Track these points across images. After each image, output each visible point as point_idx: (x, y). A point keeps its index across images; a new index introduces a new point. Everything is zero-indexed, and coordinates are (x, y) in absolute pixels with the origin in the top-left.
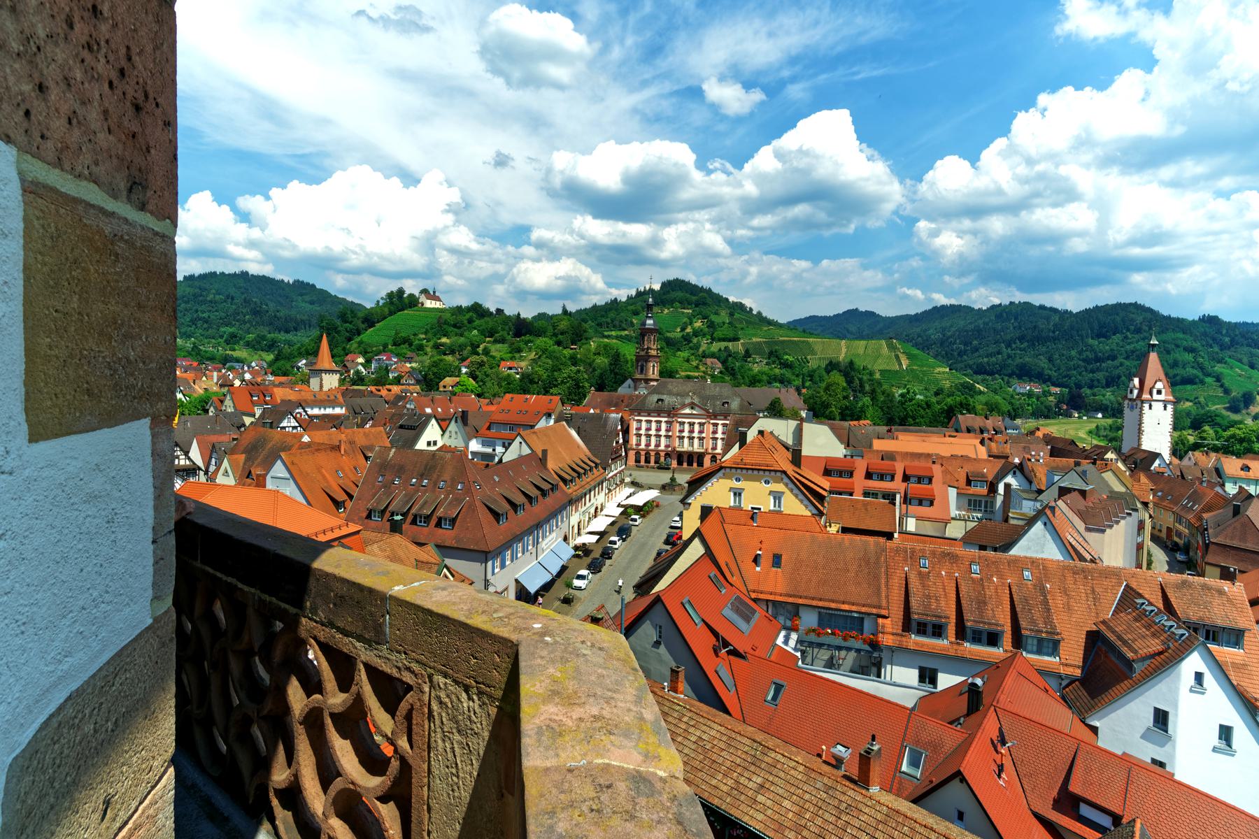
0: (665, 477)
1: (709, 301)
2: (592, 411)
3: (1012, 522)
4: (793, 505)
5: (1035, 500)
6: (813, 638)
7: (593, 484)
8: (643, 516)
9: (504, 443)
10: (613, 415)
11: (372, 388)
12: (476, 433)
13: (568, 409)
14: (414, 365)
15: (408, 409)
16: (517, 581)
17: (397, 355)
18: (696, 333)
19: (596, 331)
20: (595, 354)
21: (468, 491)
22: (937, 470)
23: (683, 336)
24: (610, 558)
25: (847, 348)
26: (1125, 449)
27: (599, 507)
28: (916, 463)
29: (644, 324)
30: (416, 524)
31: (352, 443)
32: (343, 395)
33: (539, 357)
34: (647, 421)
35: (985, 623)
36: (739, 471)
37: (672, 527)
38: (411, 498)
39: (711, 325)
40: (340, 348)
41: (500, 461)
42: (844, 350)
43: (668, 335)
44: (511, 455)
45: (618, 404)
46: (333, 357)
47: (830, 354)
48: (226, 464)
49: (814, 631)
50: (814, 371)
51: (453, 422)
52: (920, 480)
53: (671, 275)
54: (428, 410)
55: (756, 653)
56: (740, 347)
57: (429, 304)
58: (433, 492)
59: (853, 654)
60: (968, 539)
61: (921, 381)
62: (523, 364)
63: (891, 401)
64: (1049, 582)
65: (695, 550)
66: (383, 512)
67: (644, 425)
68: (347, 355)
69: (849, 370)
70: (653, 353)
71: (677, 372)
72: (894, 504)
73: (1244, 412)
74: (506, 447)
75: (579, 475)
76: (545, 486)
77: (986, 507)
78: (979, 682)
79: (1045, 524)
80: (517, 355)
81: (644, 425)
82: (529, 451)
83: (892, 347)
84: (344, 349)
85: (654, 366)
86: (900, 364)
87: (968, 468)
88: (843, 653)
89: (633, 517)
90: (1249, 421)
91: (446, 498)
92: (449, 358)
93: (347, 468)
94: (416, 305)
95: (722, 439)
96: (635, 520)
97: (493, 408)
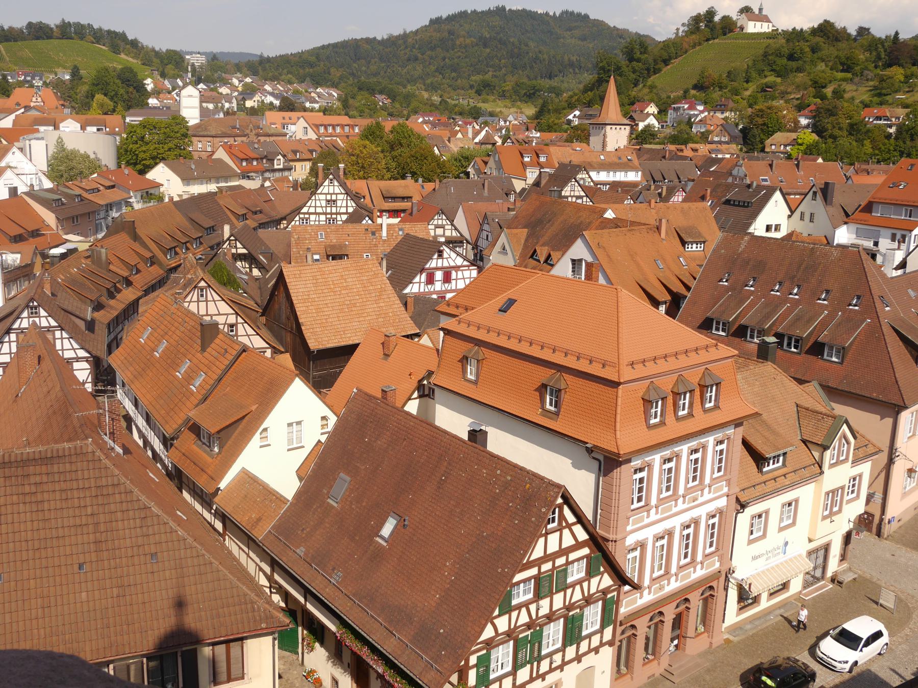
11: (672, 147)
12: (847, 217)
15: (735, 178)
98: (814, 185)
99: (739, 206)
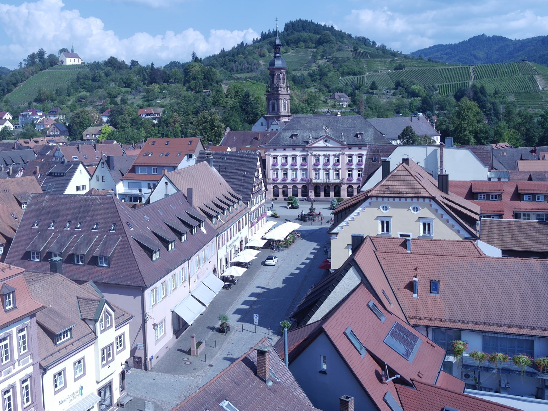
2: (229, 150)
9: (149, 184)
11: (21, 141)
15: (56, 158)
17: (43, 110)
27: (244, 241)
36: (386, 200)
41: (148, 202)
55: (423, 380)
74: (153, 187)
82: (174, 191)
85: (284, 103)
98: (101, 158)
99: (58, 176)
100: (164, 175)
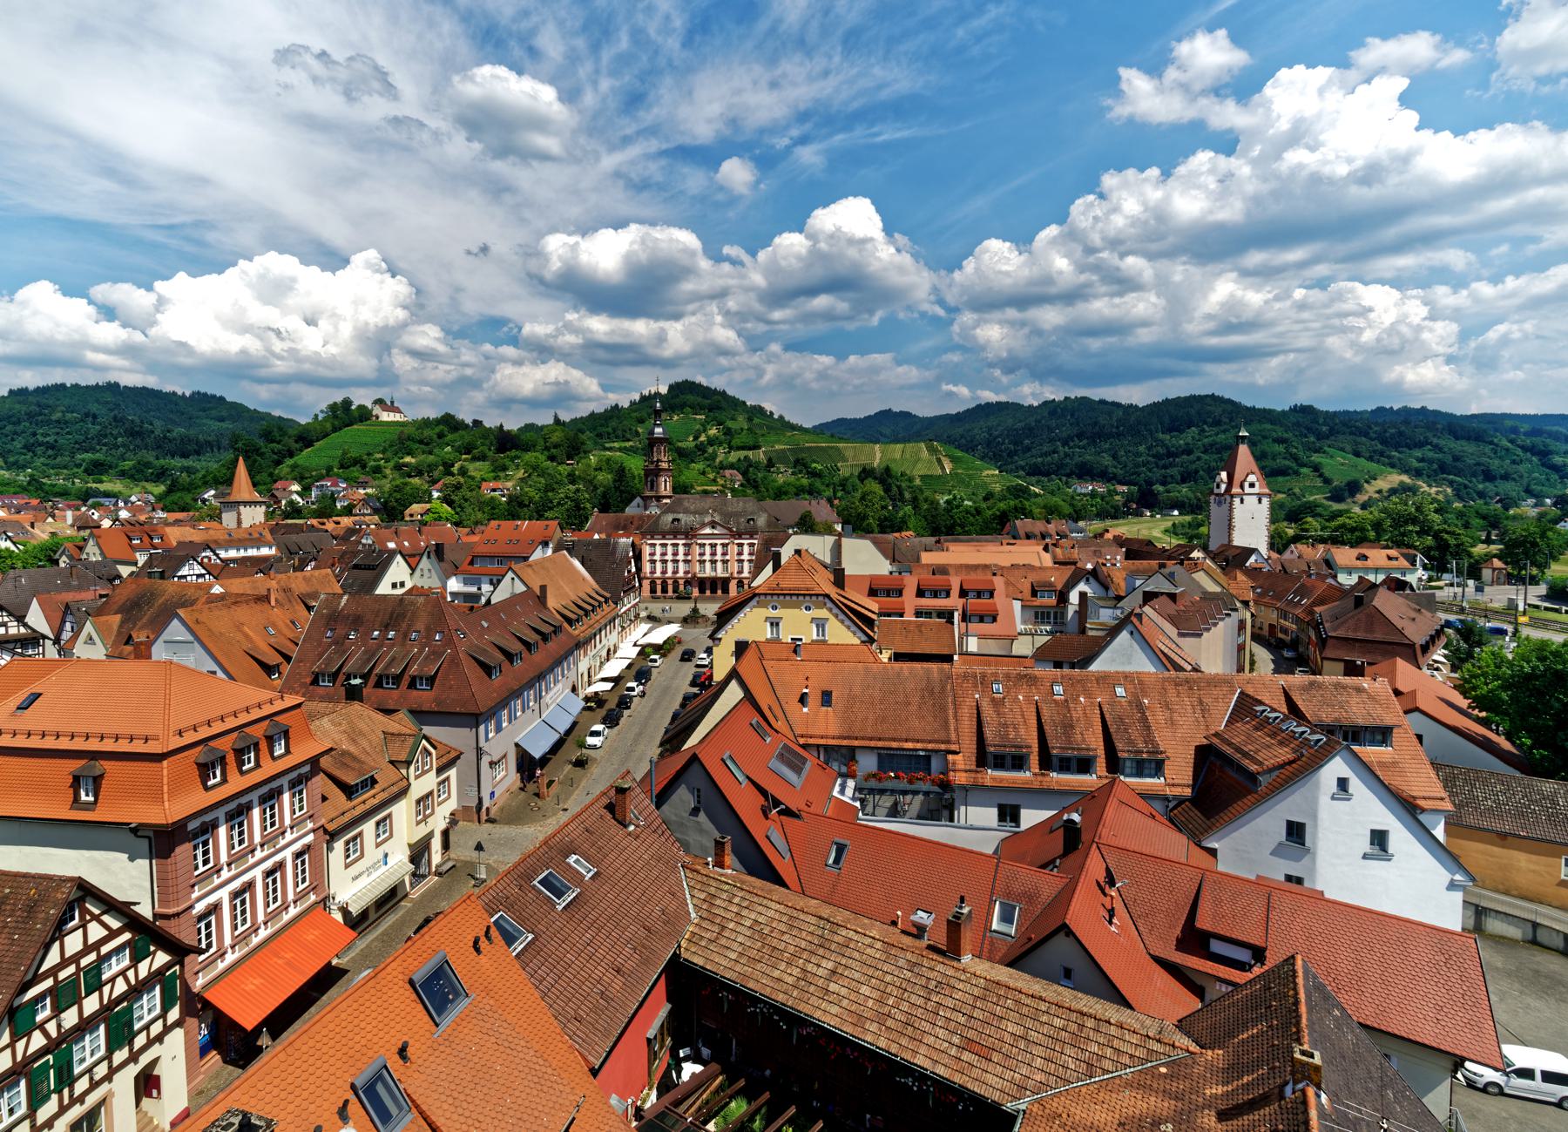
0: (685, 608)
1: (724, 404)
2: (596, 536)
3: (1091, 633)
4: (840, 633)
5: (1115, 607)
6: (873, 784)
7: (603, 622)
8: (663, 656)
10: (623, 540)
11: (314, 522)
12: (455, 570)
13: (569, 536)
14: (369, 491)
15: (364, 545)
16: (517, 745)
17: (346, 480)
18: (711, 442)
19: (596, 443)
20: (596, 470)
21: (449, 641)
22: (999, 582)
23: (696, 446)
24: (629, 708)
25: (882, 452)
26: (1213, 546)
28: (973, 576)
29: (652, 432)
30: (382, 687)
31: (286, 591)
32: (272, 531)
33: (529, 476)
34: (662, 545)
35: (1073, 749)
36: (775, 598)
37: (698, 666)
38: (373, 655)
39: (728, 432)
40: (264, 475)
41: (488, 602)
42: (878, 455)
43: (680, 444)
44: (501, 595)
45: (626, 527)
46: (255, 485)
47: (863, 460)
48: (88, 628)
49: (874, 776)
50: (846, 479)
51: (425, 558)
52: (979, 594)
53: (679, 376)
54: (391, 545)
55: (811, 810)
56: (762, 456)
57: (386, 417)
58: (403, 645)
59: (920, 797)
60: (1041, 655)
61: (968, 486)
62: (509, 484)
63: (936, 509)
64: (1147, 697)
65: (733, 693)
66: (334, 677)
67: (658, 550)
68: (275, 481)
69: (885, 476)
70: (664, 465)
71: (692, 487)
72: (952, 623)
73: (1349, 500)
74: (495, 584)
75: (587, 613)
76: (546, 629)
77: (1055, 618)
78: (1076, 817)
79: (1132, 633)
80: (502, 474)
81: (658, 550)
82: (524, 589)
83: (932, 450)
84: (271, 475)
86: (943, 468)
87: (1033, 577)
88: (908, 798)
89: (653, 657)
90: (1357, 510)
91: (420, 652)
92: (416, 481)
93: (280, 624)
94: (368, 419)
95: (750, 561)
96: (655, 661)
97: (475, 538)
100: (510, 568)
